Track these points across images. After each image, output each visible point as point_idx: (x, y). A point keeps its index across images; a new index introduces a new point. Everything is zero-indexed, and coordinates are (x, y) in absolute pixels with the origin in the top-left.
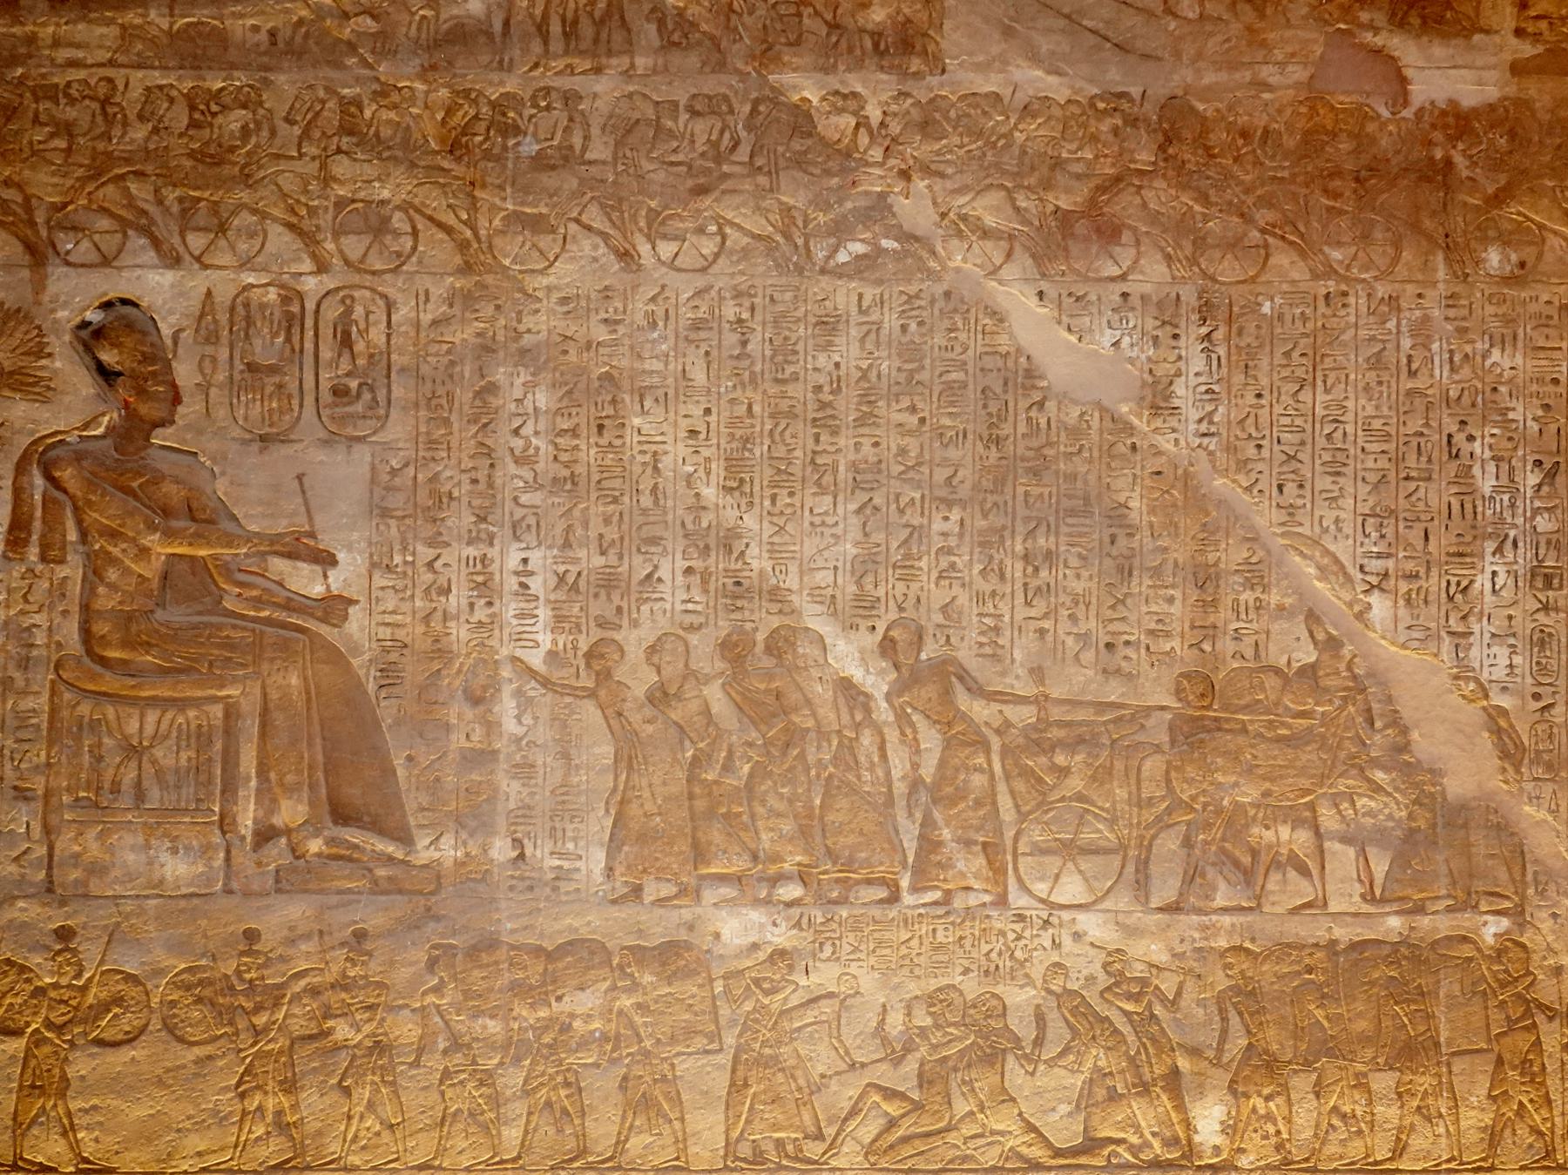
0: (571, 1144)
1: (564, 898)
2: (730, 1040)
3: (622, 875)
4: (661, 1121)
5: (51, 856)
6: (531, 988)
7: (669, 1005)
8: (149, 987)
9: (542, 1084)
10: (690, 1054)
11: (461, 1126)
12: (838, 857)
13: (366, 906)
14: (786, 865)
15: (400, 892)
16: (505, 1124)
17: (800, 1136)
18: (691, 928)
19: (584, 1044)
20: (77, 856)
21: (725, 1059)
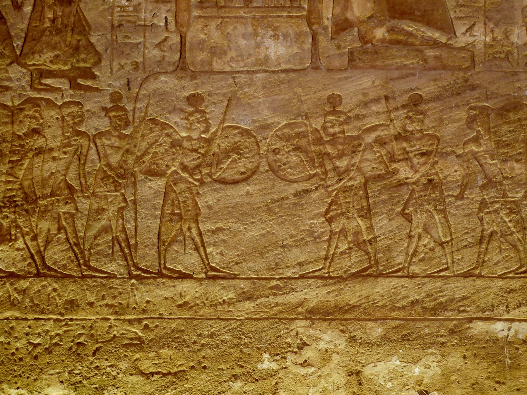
5: (182, 43)
8: (259, 137)
11: (495, 244)
13: (420, 78)
15: (444, 67)
20: (204, 41)
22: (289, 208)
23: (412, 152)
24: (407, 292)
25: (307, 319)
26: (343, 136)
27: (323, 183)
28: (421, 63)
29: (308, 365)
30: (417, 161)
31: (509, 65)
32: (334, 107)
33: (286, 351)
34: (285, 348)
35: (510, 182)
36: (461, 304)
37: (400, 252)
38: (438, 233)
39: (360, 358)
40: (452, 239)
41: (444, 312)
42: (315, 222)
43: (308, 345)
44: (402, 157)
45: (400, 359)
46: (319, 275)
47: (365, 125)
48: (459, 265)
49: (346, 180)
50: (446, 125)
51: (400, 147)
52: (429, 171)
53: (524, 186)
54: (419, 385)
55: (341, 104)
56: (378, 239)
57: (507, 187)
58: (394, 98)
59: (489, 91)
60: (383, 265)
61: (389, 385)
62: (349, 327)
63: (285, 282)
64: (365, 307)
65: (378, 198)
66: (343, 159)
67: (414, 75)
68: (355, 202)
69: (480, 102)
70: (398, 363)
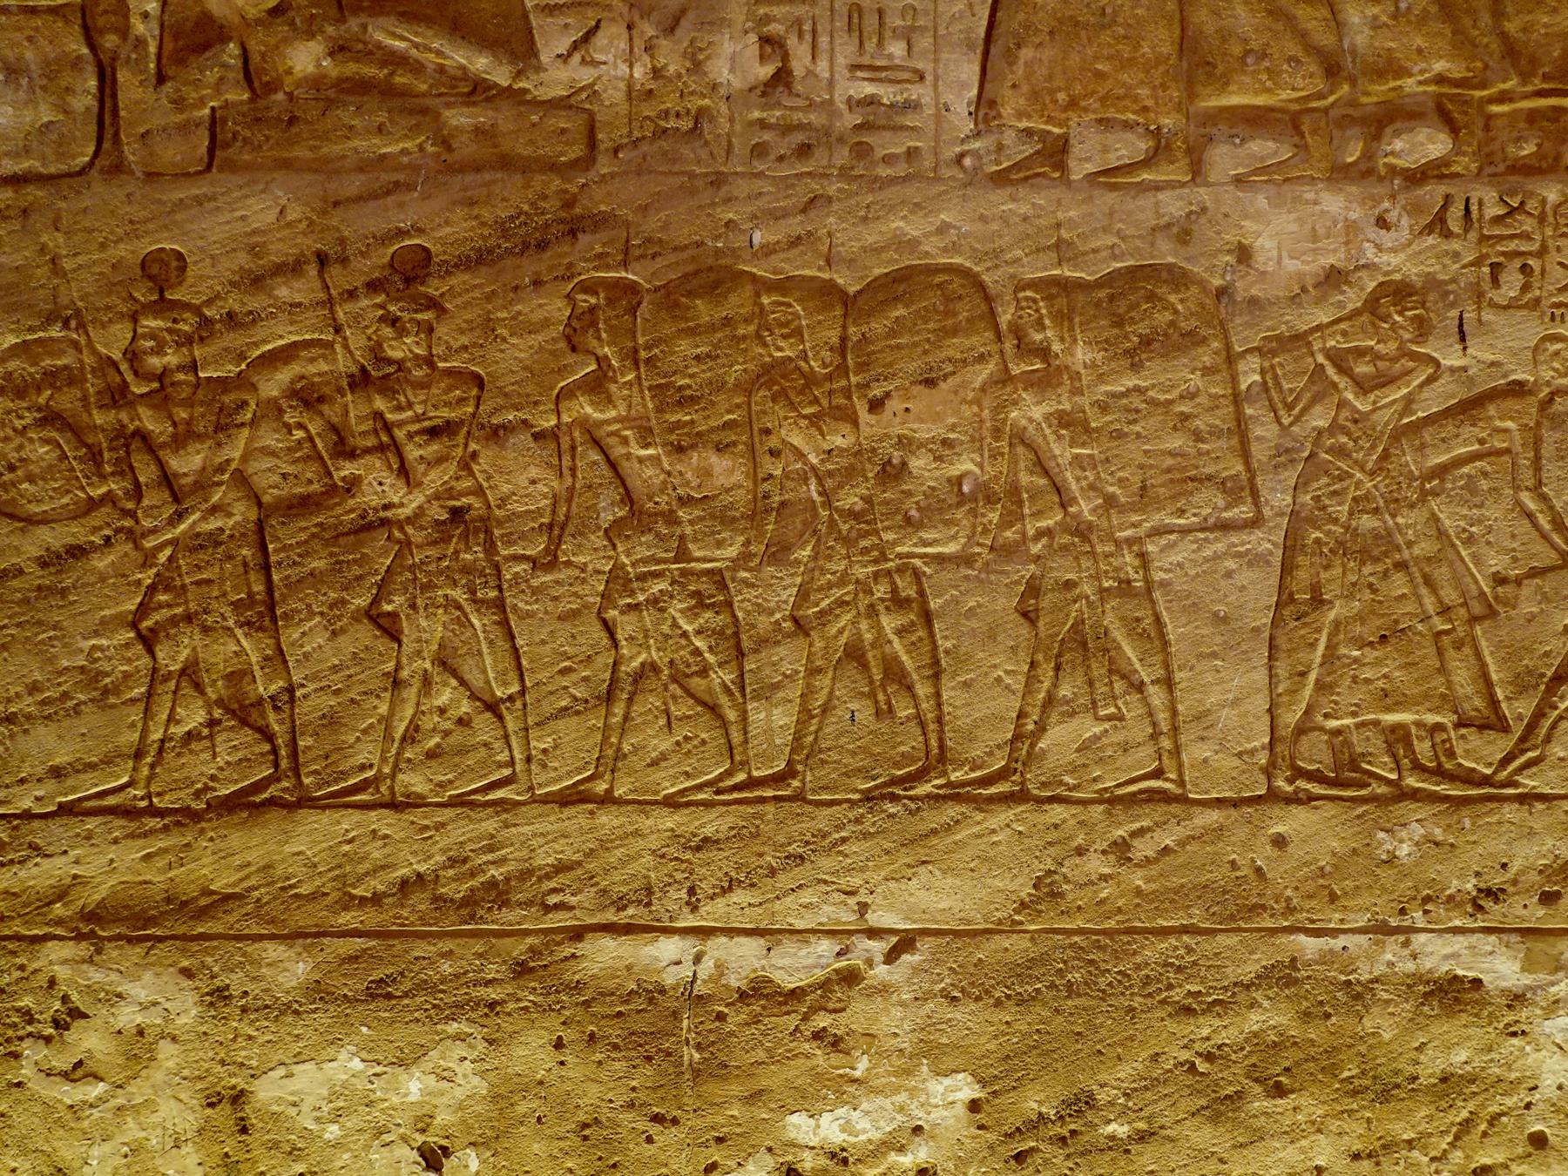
0: (911, 742)
1: (884, 171)
2: (1277, 498)
3: (1020, 115)
4: (1119, 686)
6: (811, 380)
7: (1134, 415)
9: (841, 603)
10: (1185, 531)
11: (654, 701)
12: (1534, 61)
13: (426, 197)
14: (1409, 84)
15: (506, 163)
16: (757, 697)
17: (1446, 719)
18: (1184, 236)
19: (934, 510)
21: (1268, 541)
22: (26, 601)
23: (401, 424)
24: (387, 850)
25: (80, 937)
26: (191, 378)
27: (128, 523)
28: (430, 149)
29: (85, 1076)
30: (417, 453)
31: (704, 154)
32: (161, 292)
33: (21, 1033)
34: (14, 1026)
35: (698, 513)
36: (552, 884)
37: (365, 732)
38: (484, 672)
39: (244, 1053)
40: (523, 692)
41: (499, 908)
42: (105, 642)
43: (85, 1016)
44: (371, 442)
45: (364, 1055)
46: (118, 806)
47: (256, 345)
48: (545, 766)
49: (197, 515)
50: (504, 340)
51: (365, 410)
52: (453, 483)
53: (743, 524)
54: (423, 1131)
55: (180, 283)
56: (298, 694)
57: (688, 530)
58: (344, 261)
59: (637, 234)
60: (315, 772)
61: (333, 1131)
62: (209, 960)
63: (16, 828)
64: (259, 900)
65: (298, 569)
66: (190, 449)
67: (410, 187)
68: (228, 582)
69: (608, 268)
70: (356, 1064)
